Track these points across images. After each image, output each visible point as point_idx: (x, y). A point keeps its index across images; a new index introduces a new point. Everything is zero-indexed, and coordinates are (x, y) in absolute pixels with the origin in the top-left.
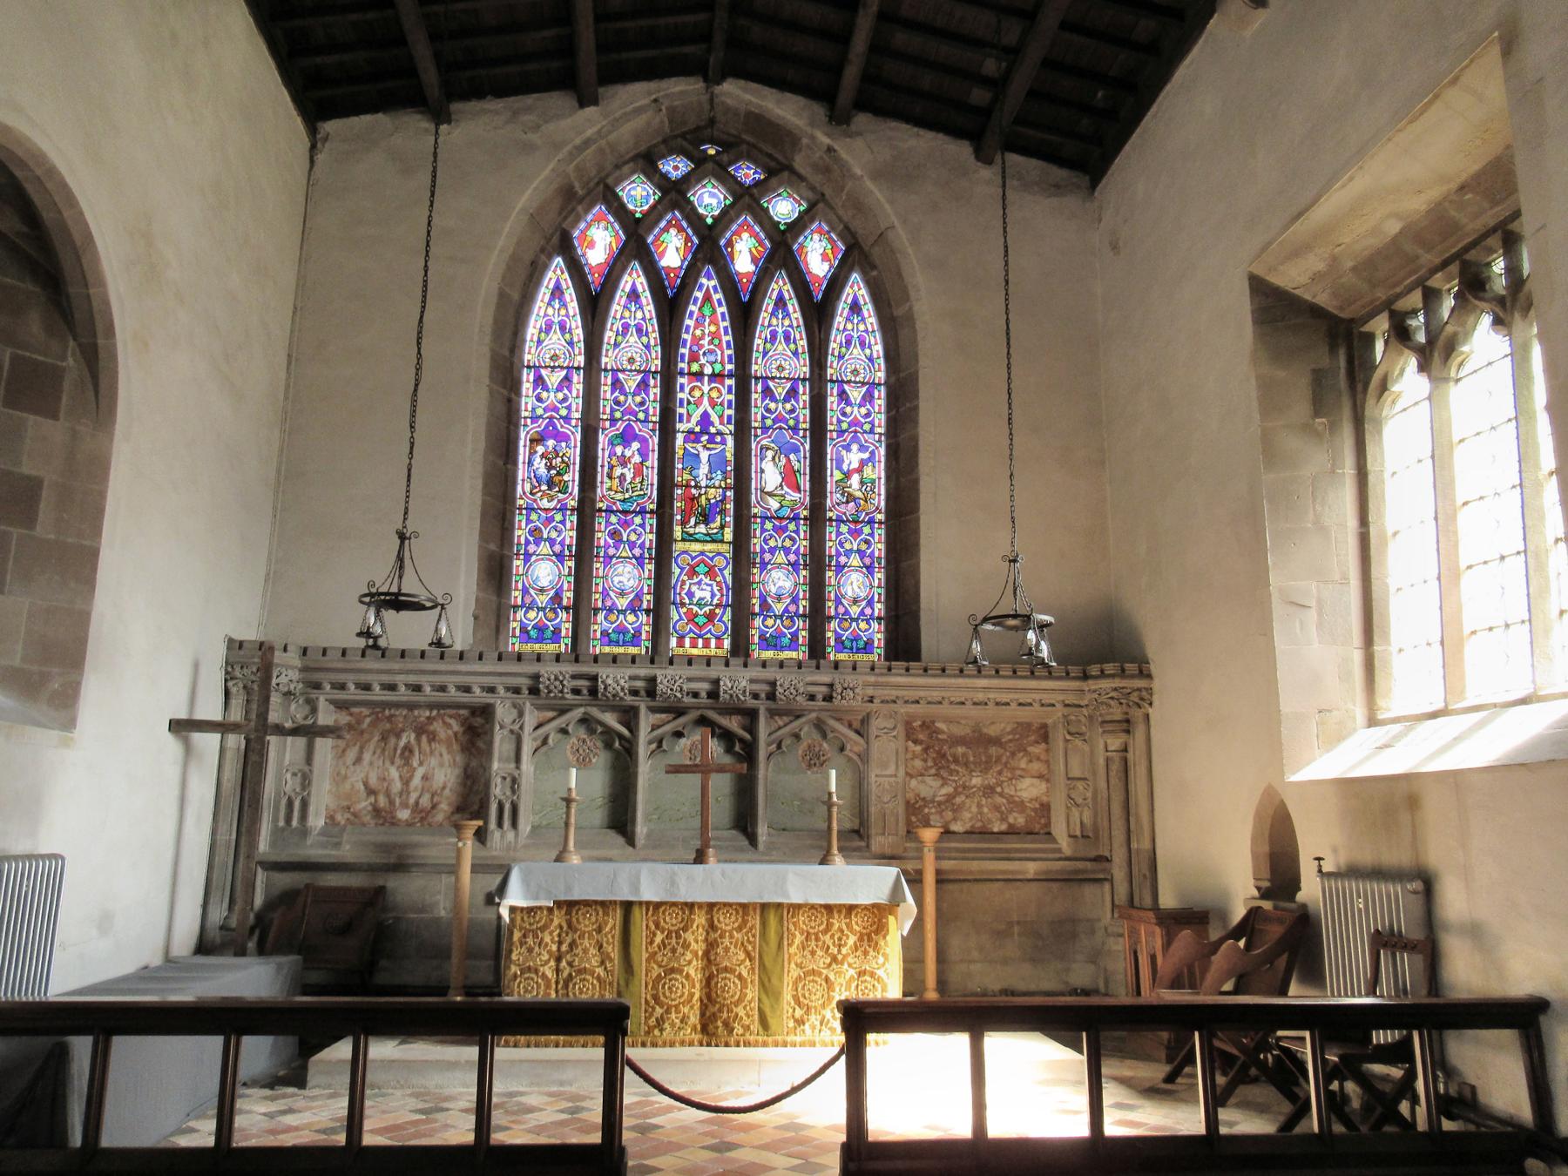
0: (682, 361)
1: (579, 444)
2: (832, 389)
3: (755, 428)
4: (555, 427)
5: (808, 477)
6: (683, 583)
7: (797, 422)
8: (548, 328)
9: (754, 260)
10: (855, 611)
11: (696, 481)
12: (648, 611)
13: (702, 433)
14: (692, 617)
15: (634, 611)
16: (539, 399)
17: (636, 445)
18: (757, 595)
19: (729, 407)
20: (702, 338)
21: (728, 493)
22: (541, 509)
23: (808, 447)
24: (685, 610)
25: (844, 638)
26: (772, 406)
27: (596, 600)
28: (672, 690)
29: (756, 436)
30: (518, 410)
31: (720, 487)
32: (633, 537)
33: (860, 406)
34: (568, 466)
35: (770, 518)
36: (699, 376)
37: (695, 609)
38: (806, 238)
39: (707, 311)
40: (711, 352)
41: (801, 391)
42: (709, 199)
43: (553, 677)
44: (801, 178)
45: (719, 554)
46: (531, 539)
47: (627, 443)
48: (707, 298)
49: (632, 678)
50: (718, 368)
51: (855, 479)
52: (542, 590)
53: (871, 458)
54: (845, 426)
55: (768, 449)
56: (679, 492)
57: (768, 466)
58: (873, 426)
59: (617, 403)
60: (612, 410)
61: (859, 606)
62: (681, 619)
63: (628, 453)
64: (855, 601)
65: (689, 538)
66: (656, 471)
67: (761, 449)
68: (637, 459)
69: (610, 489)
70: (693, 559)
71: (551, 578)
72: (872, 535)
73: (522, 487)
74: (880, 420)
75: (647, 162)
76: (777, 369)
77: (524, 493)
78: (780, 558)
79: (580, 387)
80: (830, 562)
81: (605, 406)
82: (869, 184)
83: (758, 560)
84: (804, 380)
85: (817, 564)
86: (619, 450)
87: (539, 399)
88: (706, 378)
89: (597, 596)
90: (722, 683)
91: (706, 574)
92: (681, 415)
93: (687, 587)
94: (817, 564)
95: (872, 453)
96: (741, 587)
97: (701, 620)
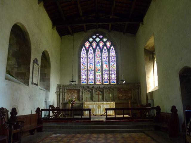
10: (113, 79)
14: (98, 80)
17: (92, 64)
36: (97, 57)
42: (98, 40)
47: (91, 64)
51: (113, 66)
57: (104, 65)
65: (97, 73)
85: (109, 74)
94: (109, 74)
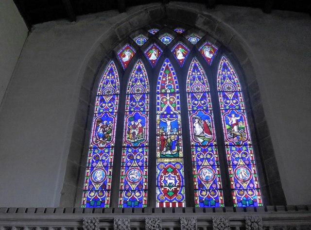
0: (158, 89)
1: (116, 121)
2: (220, 94)
3: (190, 111)
4: (107, 116)
5: (214, 128)
6: (162, 176)
7: (207, 108)
8: (107, 83)
9: (184, 55)
10: (245, 185)
11: (165, 133)
12: (145, 190)
13: (167, 114)
14: (166, 192)
15: (139, 191)
16: (102, 106)
17: (139, 121)
18: (197, 180)
19: (178, 103)
20: (166, 81)
21: (180, 137)
22: (99, 148)
23: (213, 117)
24: (163, 189)
25: (242, 199)
26: (196, 102)
27: (122, 186)
28: (154, 227)
29: (190, 114)
30: (93, 110)
31: (176, 134)
32: (138, 158)
33: (233, 100)
34: (112, 130)
35: (199, 146)
36: (165, 94)
37: (168, 188)
38: (203, 47)
39: (167, 72)
40: (169, 85)
41: (207, 96)
42: (166, 39)
43: (89, 221)
44: (199, 29)
45: (177, 163)
46: (94, 160)
47: (135, 119)
48: (167, 68)
49: (133, 221)
50: (172, 90)
51: (235, 128)
52: (98, 183)
53: (241, 119)
54: (227, 107)
55: (196, 118)
56: (158, 137)
57: (197, 125)
58: (240, 107)
59: (132, 105)
60: (130, 108)
61: (246, 183)
62: (161, 193)
63: (137, 124)
64: (244, 181)
65: (163, 156)
66: (148, 130)
67: (193, 118)
68: (140, 125)
69: (129, 138)
70: (165, 165)
71: (102, 177)
72: (247, 150)
73: (93, 139)
74: (242, 104)
75: (144, 30)
76: (197, 89)
77: (93, 142)
78: (206, 163)
79: (118, 101)
80: (229, 164)
81: (127, 107)
82: (225, 24)
83: (196, 165)
84: (208, 92)
85: (224, 165)
86: (133, 123)
87: (102, 106)
88: (168, 94)
89: (122, 184)
90: (182, 222)
91: (172, 172)
92: (158, 108)
93: (163, 178)
94: (224, 165)
95: (241, 117)
96: (189, 177)
97: (171, 194)
